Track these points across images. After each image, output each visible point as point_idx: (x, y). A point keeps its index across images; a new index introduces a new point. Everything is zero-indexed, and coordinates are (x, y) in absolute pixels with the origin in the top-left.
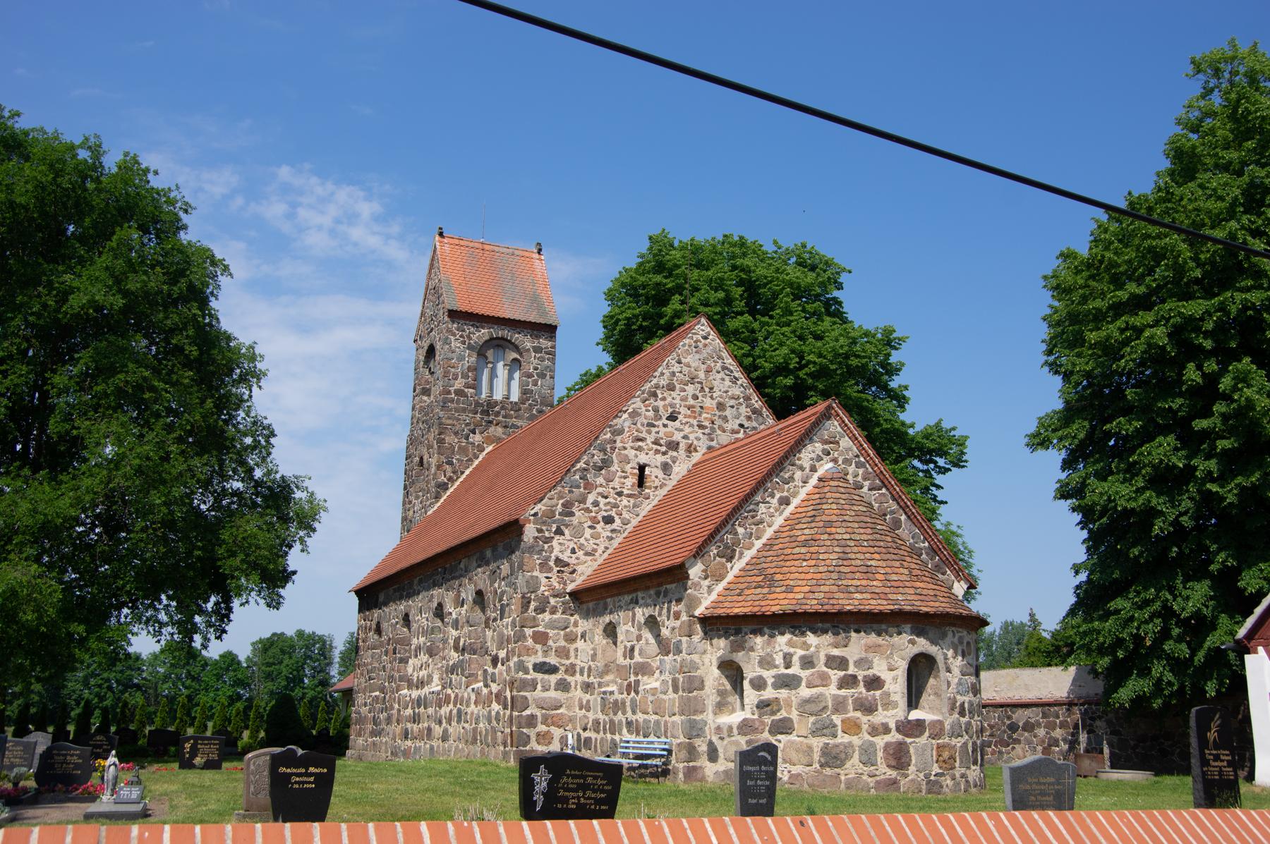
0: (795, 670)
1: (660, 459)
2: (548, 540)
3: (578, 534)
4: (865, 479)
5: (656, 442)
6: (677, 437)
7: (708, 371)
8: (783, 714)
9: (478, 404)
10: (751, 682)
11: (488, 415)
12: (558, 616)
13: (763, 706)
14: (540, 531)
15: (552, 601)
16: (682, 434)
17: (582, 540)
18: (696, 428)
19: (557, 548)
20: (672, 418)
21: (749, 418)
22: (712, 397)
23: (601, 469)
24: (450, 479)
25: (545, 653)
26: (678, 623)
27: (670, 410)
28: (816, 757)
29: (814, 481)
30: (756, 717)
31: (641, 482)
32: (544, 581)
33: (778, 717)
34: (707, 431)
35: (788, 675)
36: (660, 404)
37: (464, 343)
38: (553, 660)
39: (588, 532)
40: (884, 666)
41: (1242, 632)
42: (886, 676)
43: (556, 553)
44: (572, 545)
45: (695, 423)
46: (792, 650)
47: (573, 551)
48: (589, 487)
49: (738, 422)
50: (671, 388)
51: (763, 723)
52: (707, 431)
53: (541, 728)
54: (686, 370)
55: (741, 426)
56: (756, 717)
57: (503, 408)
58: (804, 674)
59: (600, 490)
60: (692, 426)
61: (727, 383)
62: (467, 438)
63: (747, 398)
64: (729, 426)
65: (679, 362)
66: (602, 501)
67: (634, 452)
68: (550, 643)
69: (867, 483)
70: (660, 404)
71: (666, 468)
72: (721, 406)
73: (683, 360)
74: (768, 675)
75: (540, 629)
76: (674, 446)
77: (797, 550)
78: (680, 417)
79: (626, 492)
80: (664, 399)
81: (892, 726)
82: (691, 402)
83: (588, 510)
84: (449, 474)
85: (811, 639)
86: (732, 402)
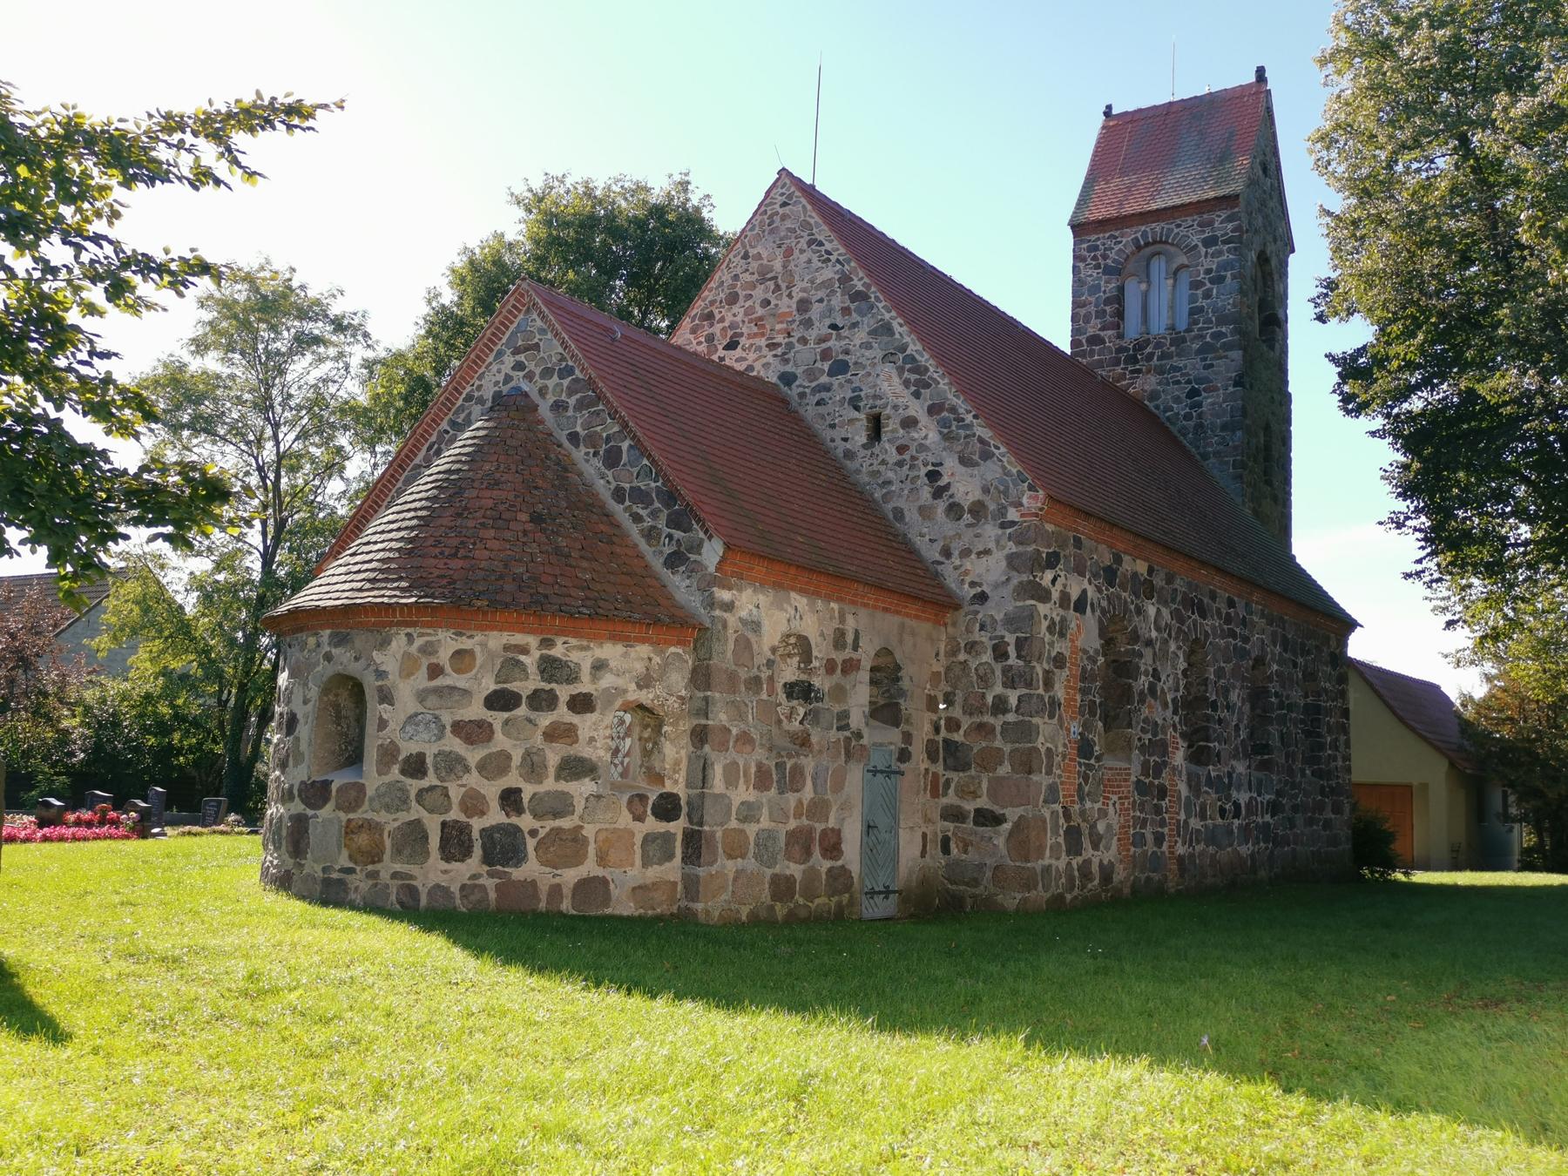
4: (570, 395)
7: (789, 253)
11: (1136, 361)
18: (765, 351)
21: (846, 311)
22: (790, 296)
27: (730, 333)
34: (779, 351)
37: (1097, 267)
45: (763, 342)
49: (828, 322)
50: (732, 299)
52: (779, 351)
55: (834, 327)
60: (759, 349)
61: (816, 263)
63: (845, 279)
64: (812, 335)
65: (746, 256)
69: (572, 401)
72: (804, 305)
73: (752, 252)
78: (743, 341)
82: (760, 311)
86: (820, 294)
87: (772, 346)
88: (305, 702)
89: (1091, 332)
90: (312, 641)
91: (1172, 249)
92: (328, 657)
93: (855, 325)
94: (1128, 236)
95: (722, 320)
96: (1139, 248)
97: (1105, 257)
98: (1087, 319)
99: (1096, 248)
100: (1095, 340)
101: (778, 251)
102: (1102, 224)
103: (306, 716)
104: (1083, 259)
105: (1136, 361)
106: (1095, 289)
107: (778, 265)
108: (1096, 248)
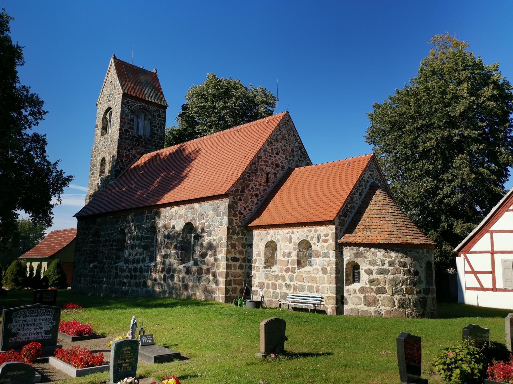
0: (386, 266)
1: (273, 171)
2: (237, 203)
3: (246, 201)
5: (272, 164)
6: (279, 162)
8: (382, 285)
9: (134, 137)
10: (365, 271)
12: (240, 236)
13: (371, 281)
14: (234, 199)
15: (238, 229)
16: (280, 161)
17: (248, 204)
19: (239, 206)
20: (277, 154)
23: (254, 173)
24: (122, 168)
25: (235, 253)
26: (326, 245)
27: (277, 150)
28: (396, 304)
29: (368, 187)
30: (368, 286)
31: (267, 181)
32: (235, 221)
33: (379, 286)
34: (288, 160)
35: (382, 269)
36: (274, 147)
37: (128, 109)
38: (238, 256)
39: (250, 200)
40: (419, 265)
41: (456, 249)
42: (420, 270)
43: (239, 209)
44: (244, 205)
46: (384, 258)
47: (245, 209)
48: (250, 181)
50: (277, 141)
51: (372, 289)
52: (288, 160)
53: (233, 286)
54: (282, 134)
56: (368, 286)
57: (144, 140)
58: (391, 268)
59: (254, 182)
62: (129, 151)
66: (254, 187)
67: (265, 167)
68: (237, 248)
70: (274, 147)
71: (275, 174)
72: (292, 151)
73: (281, 130)
74: (374, 268)
75: (234, 242)
76: (277, 165)
77: (375, 216)
78: (280, 154)
79: (262, 184)
80: (275, 145)
81: (422, 291)
83: (250, 191)
84: (121, 166)
85: (393, 254)
87: (287, 159)
88: (421, 267)
89: (126, 128)
90: (421, 251)
91: (148, 113)
92: (427, 256)
93: (303, 161)
94: (138, 104)
95: (275, 145)
96: (140, 108)
97: (131, 107)
98: (125, 123)
99: (128, 103)
100: (126, 131)
101: (287, 133)
102: (131, 97)
103: (422, 271)
104: (125, 105)
105: (138, 142)
106: (127, 115)
107: (287, 136)
108: (128, 103)
